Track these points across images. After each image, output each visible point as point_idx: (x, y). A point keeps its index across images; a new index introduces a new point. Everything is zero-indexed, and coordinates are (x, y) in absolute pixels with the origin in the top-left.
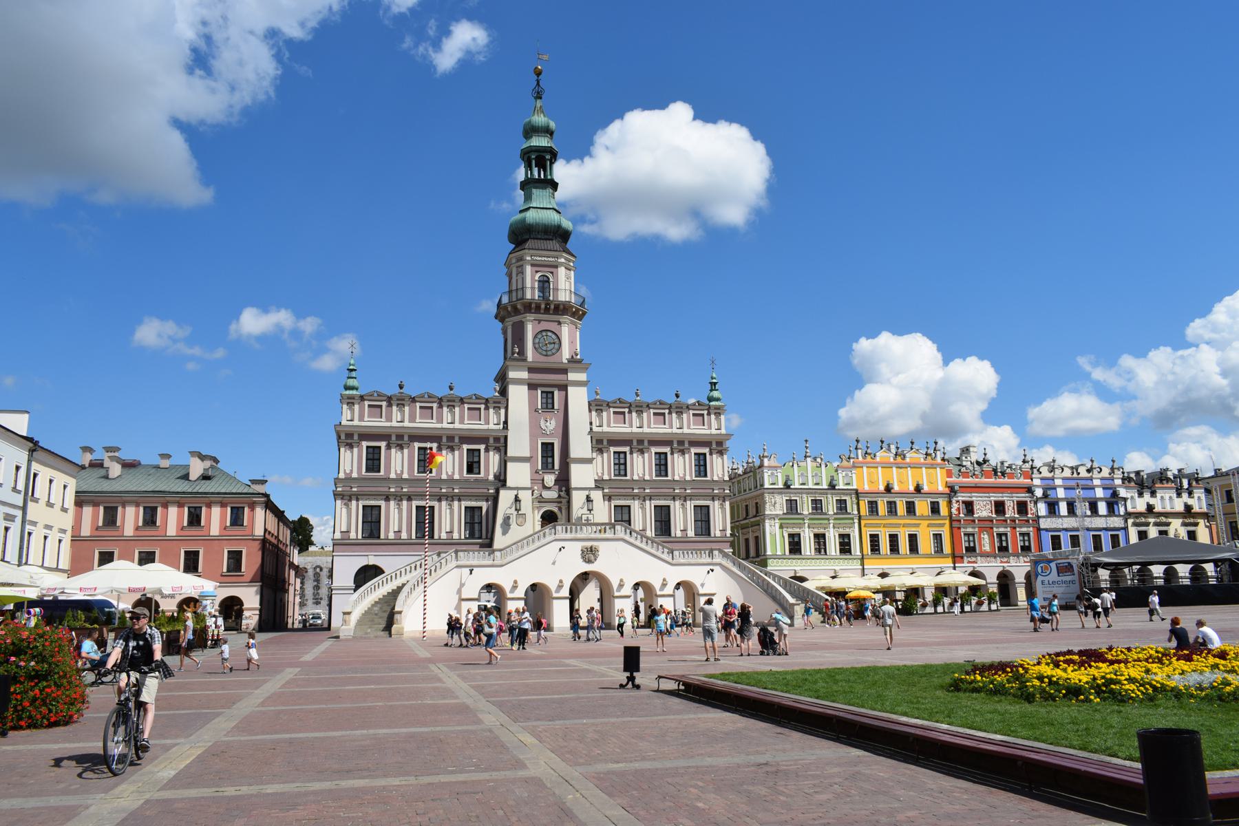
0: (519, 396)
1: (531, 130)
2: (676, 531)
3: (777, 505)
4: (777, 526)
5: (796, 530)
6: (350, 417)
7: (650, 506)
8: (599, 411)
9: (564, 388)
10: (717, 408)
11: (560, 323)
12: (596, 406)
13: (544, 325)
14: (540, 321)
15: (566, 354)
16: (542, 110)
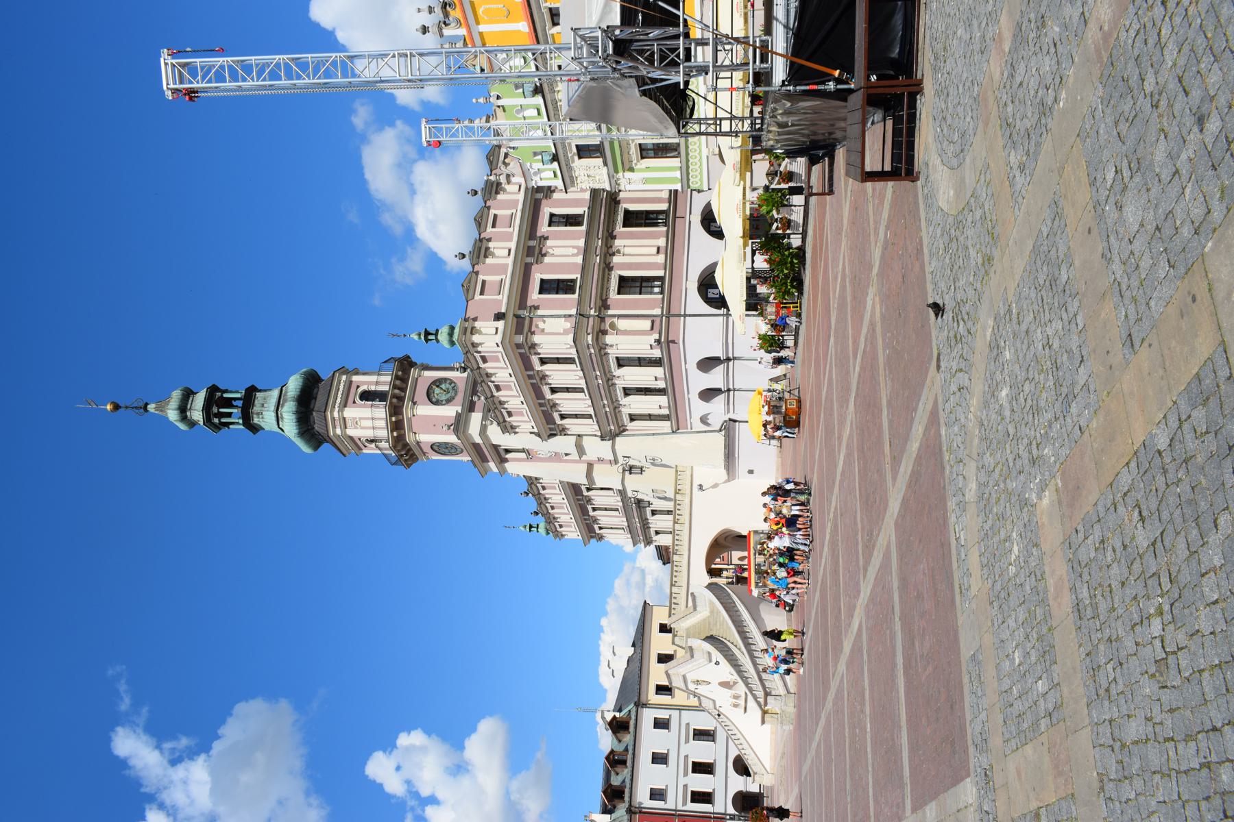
0: (517, 468)
1: (192, 424)
2: (661, 384)
3: (592, 173)
4: (628, 174)
5: (634, 152)
6: (572, 532)
7: (624, 401)
8: (512, 427)
9: (496, 447)
10: (464, 346)
11: (418, 443)
12: (507, 428)
13: (427, 449)
14: (424, 454)
15: (452, 438)
16: (161, 408)
